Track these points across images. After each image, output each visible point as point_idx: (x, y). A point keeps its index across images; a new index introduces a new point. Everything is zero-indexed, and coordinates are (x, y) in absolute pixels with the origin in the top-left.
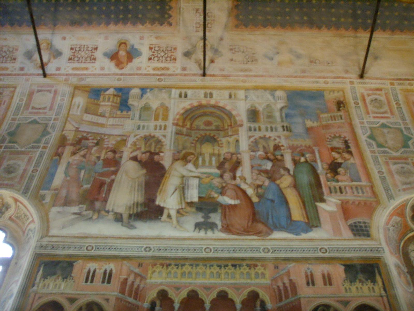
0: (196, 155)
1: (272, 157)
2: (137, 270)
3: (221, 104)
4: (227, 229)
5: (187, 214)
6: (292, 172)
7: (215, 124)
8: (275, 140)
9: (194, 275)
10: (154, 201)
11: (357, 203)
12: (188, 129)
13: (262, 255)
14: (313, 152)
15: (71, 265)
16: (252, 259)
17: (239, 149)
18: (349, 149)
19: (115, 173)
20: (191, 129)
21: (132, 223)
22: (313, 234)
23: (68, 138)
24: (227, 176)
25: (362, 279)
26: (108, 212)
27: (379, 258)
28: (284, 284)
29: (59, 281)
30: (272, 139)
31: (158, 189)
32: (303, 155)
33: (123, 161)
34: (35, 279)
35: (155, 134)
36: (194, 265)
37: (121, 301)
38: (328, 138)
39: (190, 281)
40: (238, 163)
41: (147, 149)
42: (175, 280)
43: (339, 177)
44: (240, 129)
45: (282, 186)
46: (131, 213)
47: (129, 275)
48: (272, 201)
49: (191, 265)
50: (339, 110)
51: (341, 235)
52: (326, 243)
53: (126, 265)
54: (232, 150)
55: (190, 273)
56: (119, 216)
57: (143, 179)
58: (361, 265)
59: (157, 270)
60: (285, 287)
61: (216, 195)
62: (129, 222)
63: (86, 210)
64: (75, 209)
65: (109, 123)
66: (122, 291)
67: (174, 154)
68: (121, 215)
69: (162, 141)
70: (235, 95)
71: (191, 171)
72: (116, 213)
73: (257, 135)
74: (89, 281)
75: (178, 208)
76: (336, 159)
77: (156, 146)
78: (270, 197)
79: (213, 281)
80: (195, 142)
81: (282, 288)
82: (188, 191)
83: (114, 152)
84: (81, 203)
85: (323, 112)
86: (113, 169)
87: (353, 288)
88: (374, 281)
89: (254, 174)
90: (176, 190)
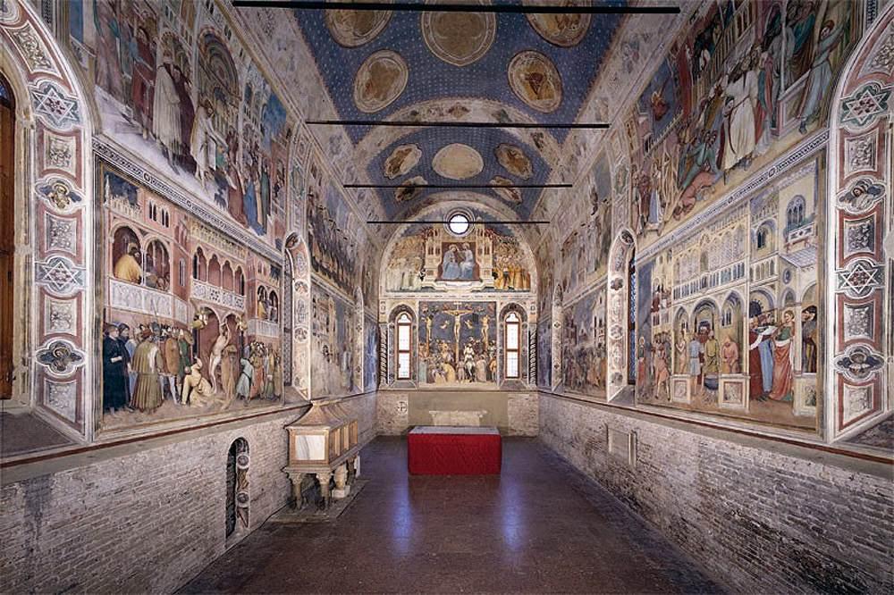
34: (105, 194)
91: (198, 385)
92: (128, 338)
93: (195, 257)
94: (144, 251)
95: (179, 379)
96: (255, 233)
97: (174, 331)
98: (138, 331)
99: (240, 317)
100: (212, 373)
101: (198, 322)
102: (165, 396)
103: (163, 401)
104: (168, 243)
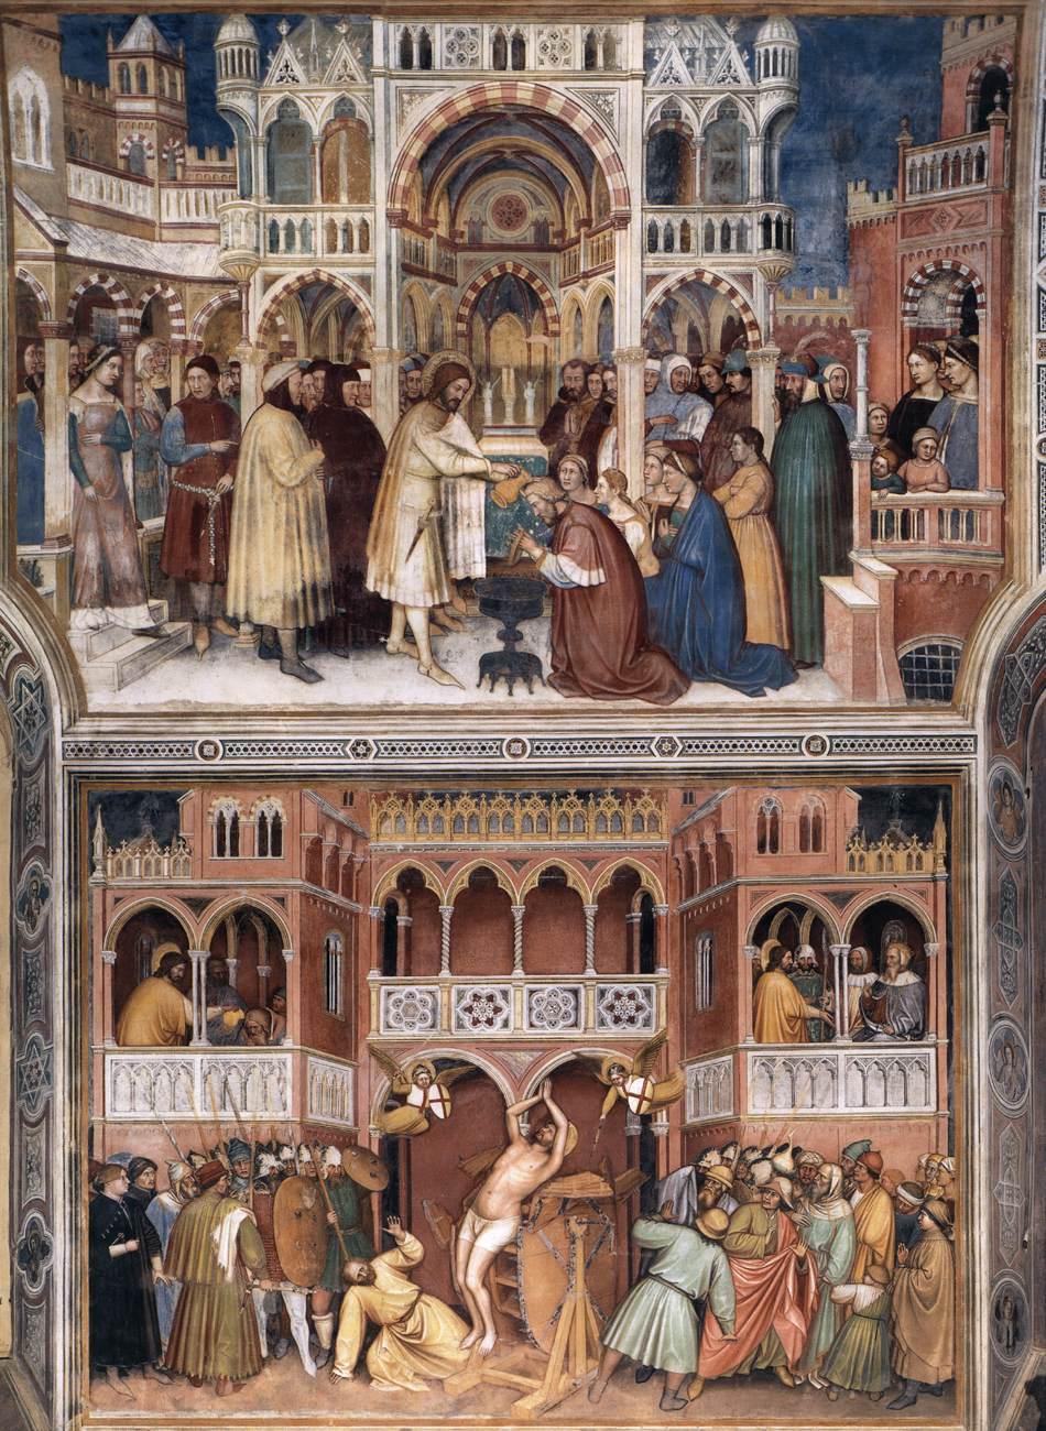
0: (473, 373)
1: (713, 383)
2: (341, 815)
3: (554, 107)
4: (568, 677)
5: (459, 626)
6: (767, 452)
7: (533, 214)
8: (733, 293)
9: (483, 825)
11: (942, 576)
12: (441, 242)
13: (657, 761)
14: (848, 359)
15: (170, 803)
16: (628, 773)
18: (974, 339)
19: (228, 462)
20: (449, 244)
21: (307, 663)
22: (791, 694)
23: (41, 297)
24: (571, 468)
25: (898, 831)
26: (235, 623)
27: (956, 770)
28: (703, 846)
29: (153, 853)
30: (723, 289)
31: (367, 528)
32: (814, 371)
33: (247, 407)
34: (92, 853)
35: (334, 271)
36: (483, 795)
37: (315, 902)
38: (911, 283)
39: (474, 842)
40: (604, 414)
41: (317, 352)
42: (439, 841)
43: (913, 470)
44: (619, 236)
45: (734, 509)
47: (322, 829)
48: (698, 570)
49: (475, 795)
50: (981, 125)
51: (874, 694)
52: (829, 721)
53: (313, 803)
54: (588, 350)
55: (473, 818)
57: (318, 488)
58: (905, 789)
59: (392, 813)
60: (705, 857)
61: (537, 552)
62: (301, 659)
63: (172, 619)
64: (137, 616)
65: (165, 219)
66: (313, 876)
67: (403, 371)
69: (361, 307)
70: (609, 53)
71: (462, 452)
72: (259, 628)
73: (679, 267)
74: (228, 851)
75: (430, 604)
76: (919, 387)
77: (342, 333)
78: (694, 555)
79: (529, 841)
80: (466, 311)
81: (696, 859)
83: (209, 364)
84: (149, 595)
85: (919, 142)
86: (219, 446)
87: (871, 858)
88: (926, 838)
89: (651, 460)
90: (420, 532)
91: (403, 1320)
92: (154, 1193)
93: (391, 908)
94: (198, 955)
95: (321, 1301)
96: (735, 698)
97: (306, 1156)
98: (181, 1171)
99: (628, 1061)
100: (471, 1277)
101: (401, 1118)
102: (271, 1348)
103: (263, 1362)
104: (281, 901)
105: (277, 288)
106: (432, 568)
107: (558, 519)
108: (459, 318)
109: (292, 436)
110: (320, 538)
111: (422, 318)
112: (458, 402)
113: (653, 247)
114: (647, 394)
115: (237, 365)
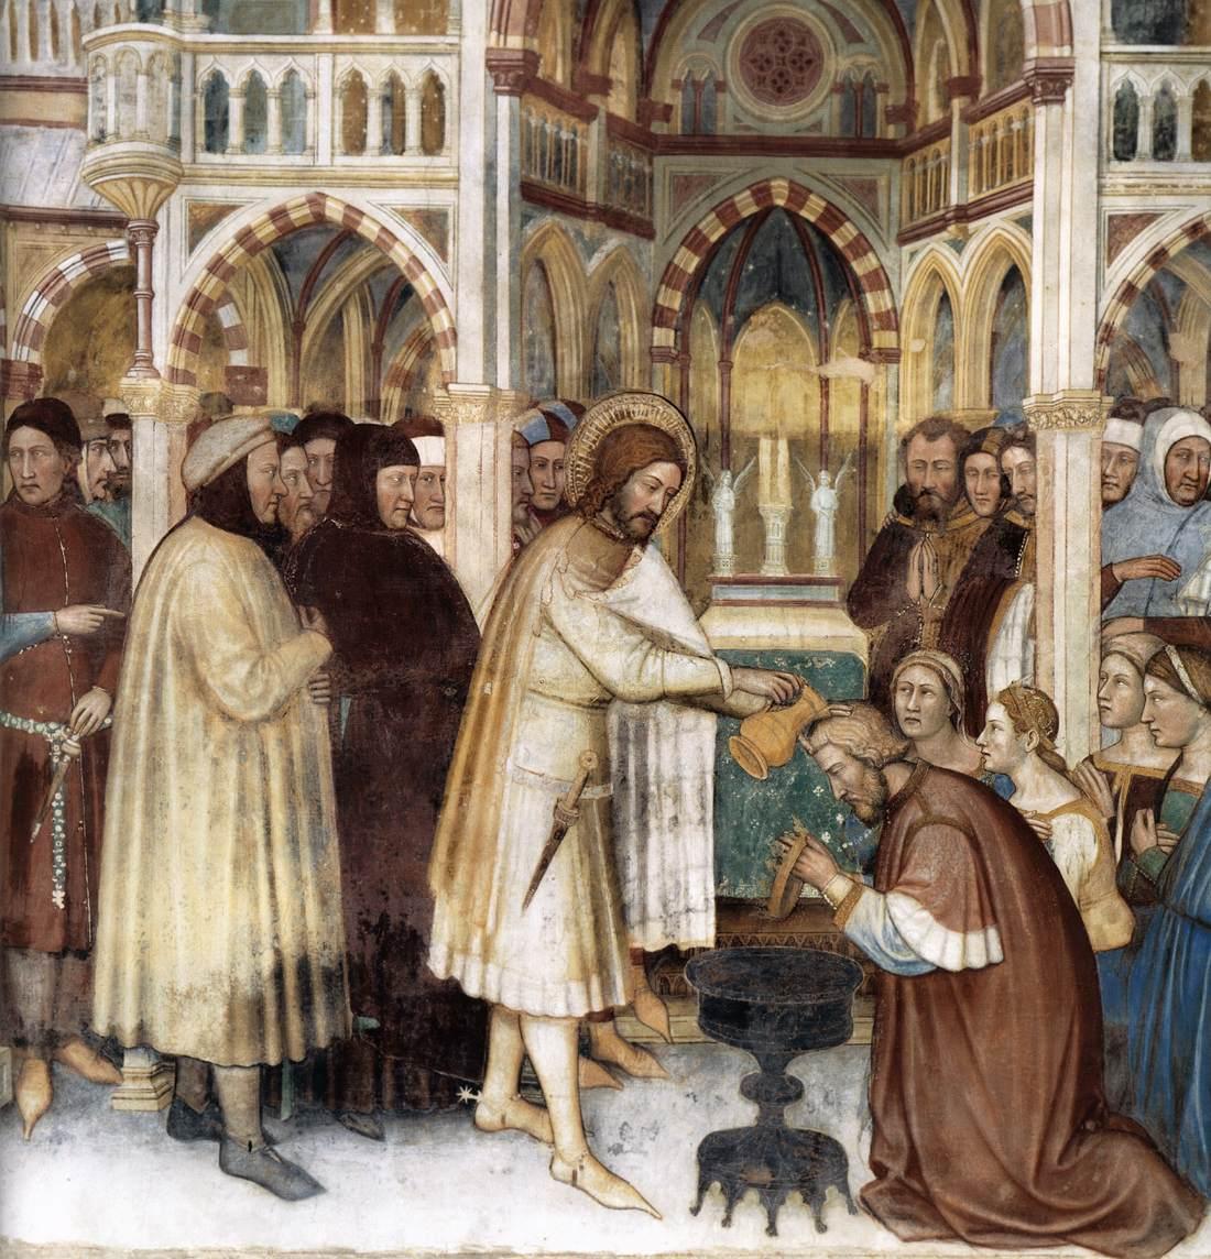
0: (689, 452)
5: (644, 1064)
10: (414, 943)
17: (1020, 383)
20: (637, 136)
21: (285, 1151)
26: (111, 1050)
35: (361, 198)
41: (316, 394)
44: (1043, 119)
46: (273, 1059)
54: (966, 397)
56: (193, 1089)
57: (313, 728)
61: (838, 887)
62: (269, 1140)
67: (523, 443)
68: (208, 1073)
69: (423, 286)
71: (659, 642)
72: (170, 1064)
75: (580, 1011)
77: (375, 351)
80: (674, 300)
82: (643, 848)
86: (76, 619)
89: (1116, 665)
90: (559, 834)
105: (221, 239)
106: (587, 921)
107: (889, 807)
108: (658, 316)
109: (255, 599)
110: (317, 846)
111: (570, 316)
112: (652, 519)
113: (1125, 148)
114: (1107, 504)
115: (122, 421)
